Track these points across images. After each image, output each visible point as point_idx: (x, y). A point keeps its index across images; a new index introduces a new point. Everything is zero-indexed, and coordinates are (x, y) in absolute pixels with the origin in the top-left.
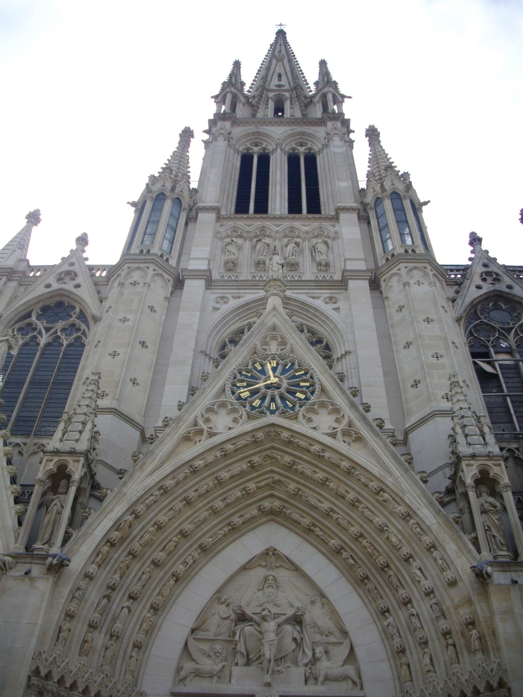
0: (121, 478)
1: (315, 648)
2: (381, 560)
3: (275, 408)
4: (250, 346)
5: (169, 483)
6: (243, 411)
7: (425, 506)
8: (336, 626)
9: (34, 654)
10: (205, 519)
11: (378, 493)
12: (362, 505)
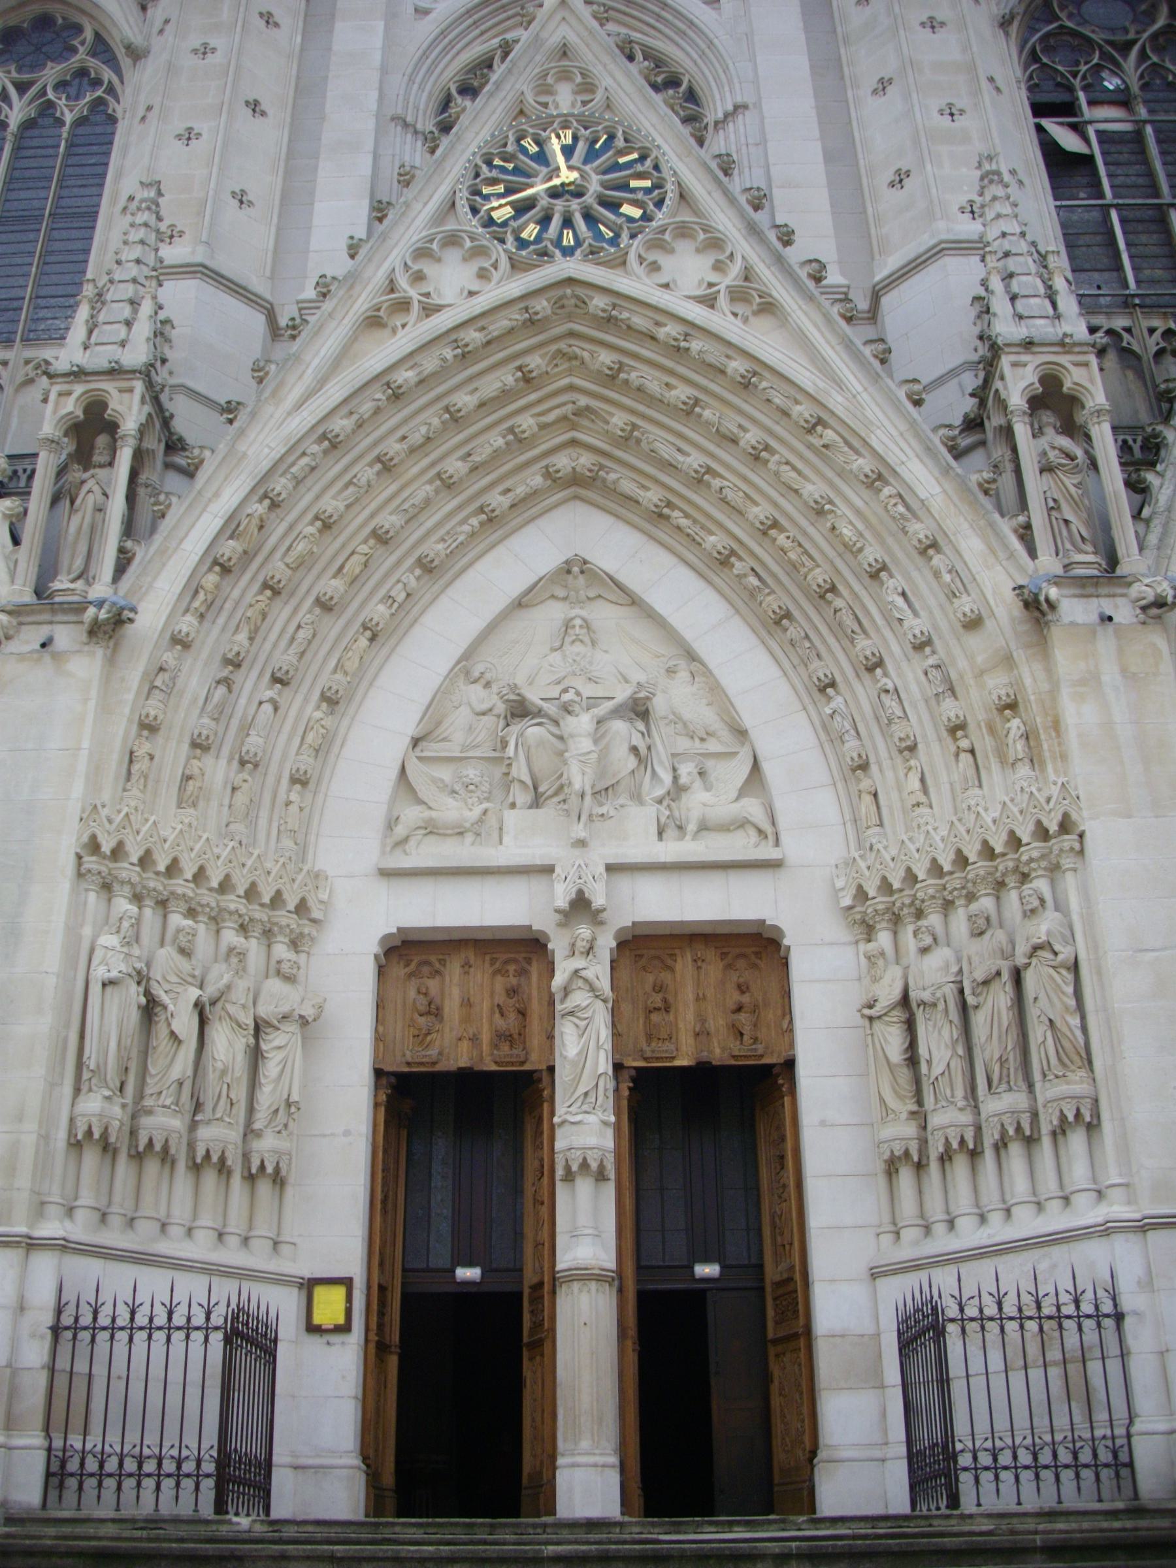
0: (231, 421)
1: (677, 765)
2: (819, 576)
3: (572, 243)
5: (341, 425)
7: (917, 456)
8: (722, 719)
9: (83, 811)
10: (427, 502)
11: (811, 430)
12: (777, 457)
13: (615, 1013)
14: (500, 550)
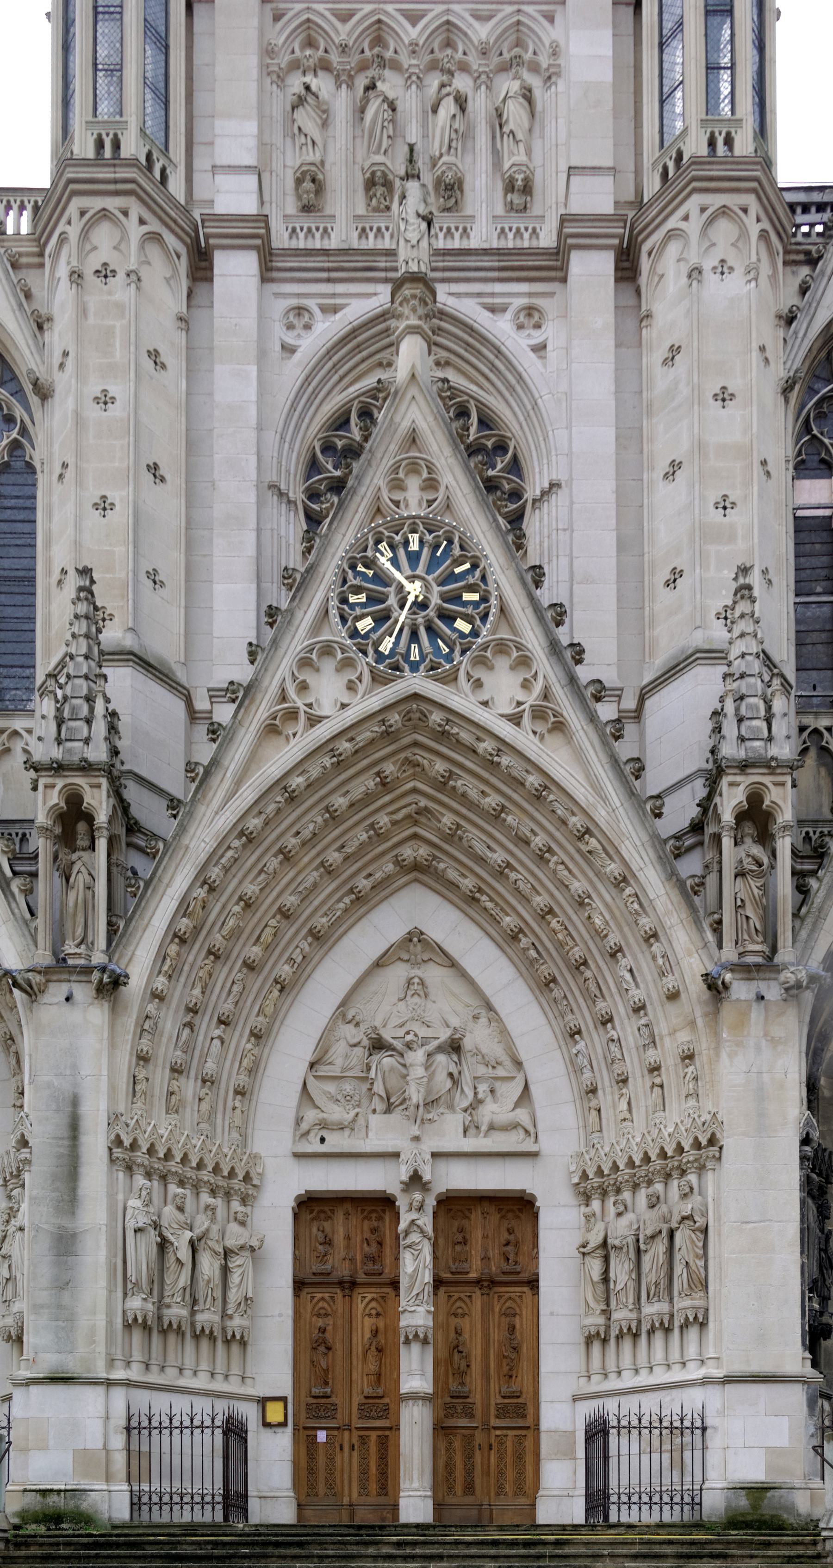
0: (175, 816)
2: (577, 953)
4: (368, 494)
9: (109, 1119)
10: (315, 885)
11: (580, 838)
13: (435, 1246)
14: (364, 921)
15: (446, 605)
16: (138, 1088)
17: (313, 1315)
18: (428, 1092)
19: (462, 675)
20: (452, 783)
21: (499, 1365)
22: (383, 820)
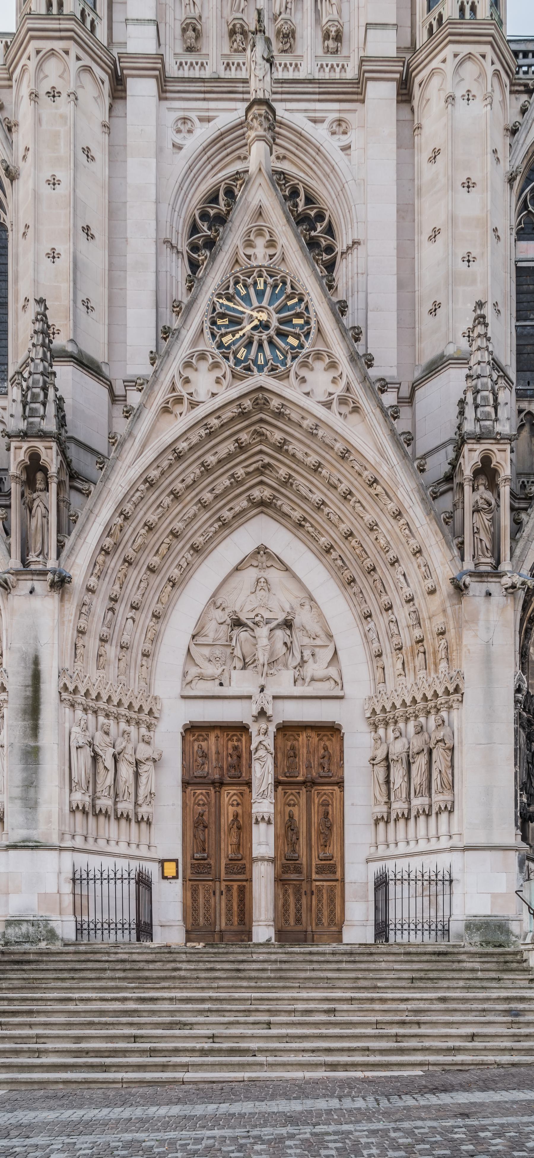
0: (101, 469)
4: (230, 251)
6: (226, 366)
9: (59, 673)
10: (195, 515)
11: (370, 486)
13: (275, 758)
14: (228, 540)
15: (282, 327)
16: (78, 651)
17: (194, 804)
18: (272, 654)
19: (292, 374)
20: (286, 447)
21: (318, 838)
22: (240, 471)
